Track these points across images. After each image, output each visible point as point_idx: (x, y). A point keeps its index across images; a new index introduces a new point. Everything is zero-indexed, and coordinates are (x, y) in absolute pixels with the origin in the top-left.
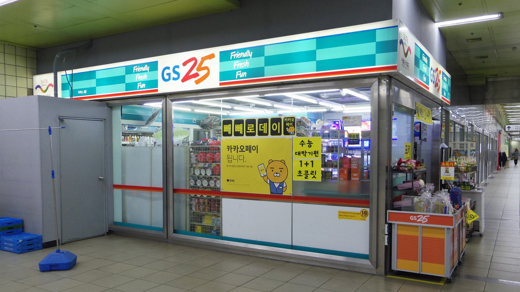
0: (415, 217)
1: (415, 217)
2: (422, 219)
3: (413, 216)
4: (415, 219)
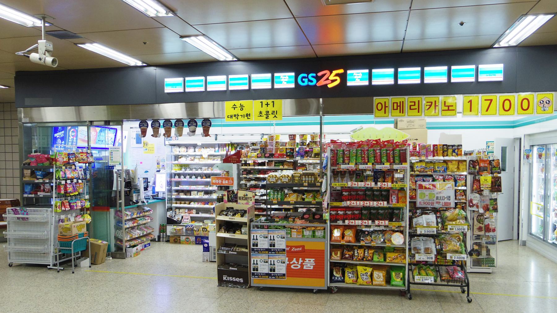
0: (312, 77)
1: (312, 77)
2: (328, 79)
3: (305, 75)
4: (312, 81)
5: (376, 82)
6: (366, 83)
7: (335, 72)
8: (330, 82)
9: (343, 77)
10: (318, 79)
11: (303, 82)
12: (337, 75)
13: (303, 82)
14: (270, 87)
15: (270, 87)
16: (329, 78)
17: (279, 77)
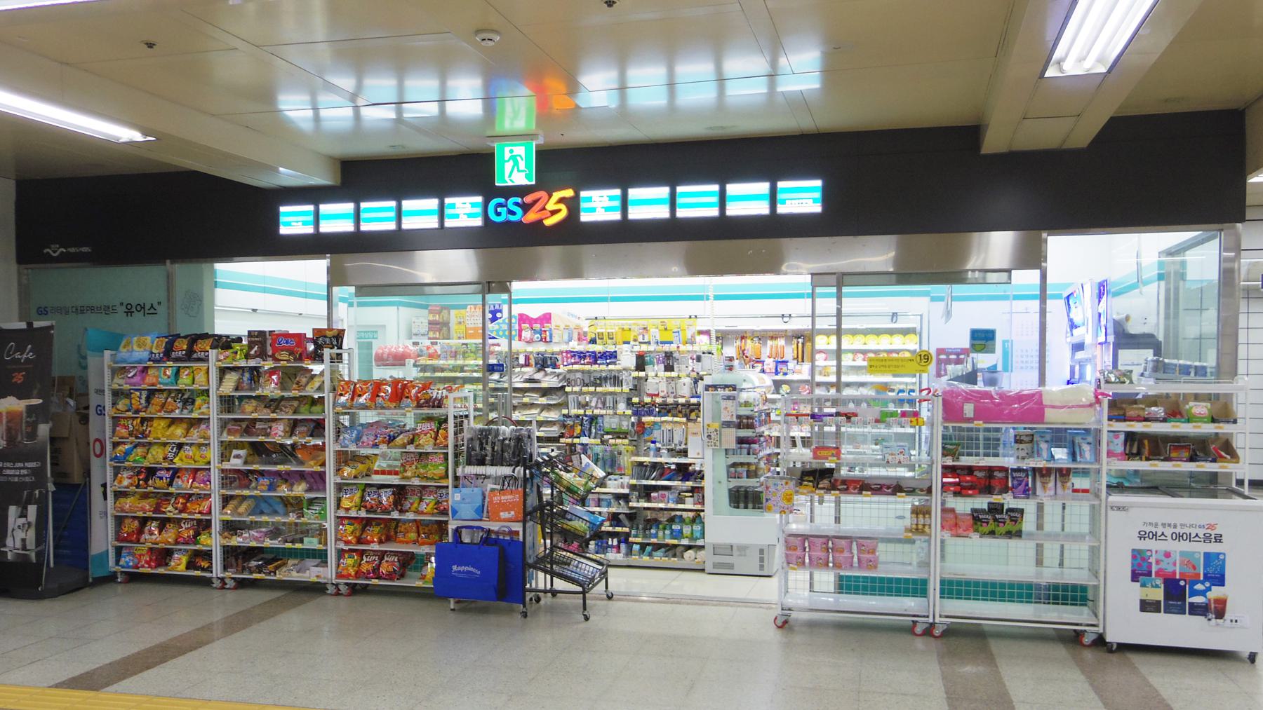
0: (516, 204)
1: (516, 204)
3: (501, 200)
4: (513, 213)
5: (635, 214)
6: (616, 216)
7: (557, 195)
8: (549, 214)
9: (573, 205)
10: (526, 208)
11: (498, 214)
12: (561, 200)
13: (498, 214)
14: (436, 225)
15: (436, 225)
16: (547, 207)
17: (453, 206)
